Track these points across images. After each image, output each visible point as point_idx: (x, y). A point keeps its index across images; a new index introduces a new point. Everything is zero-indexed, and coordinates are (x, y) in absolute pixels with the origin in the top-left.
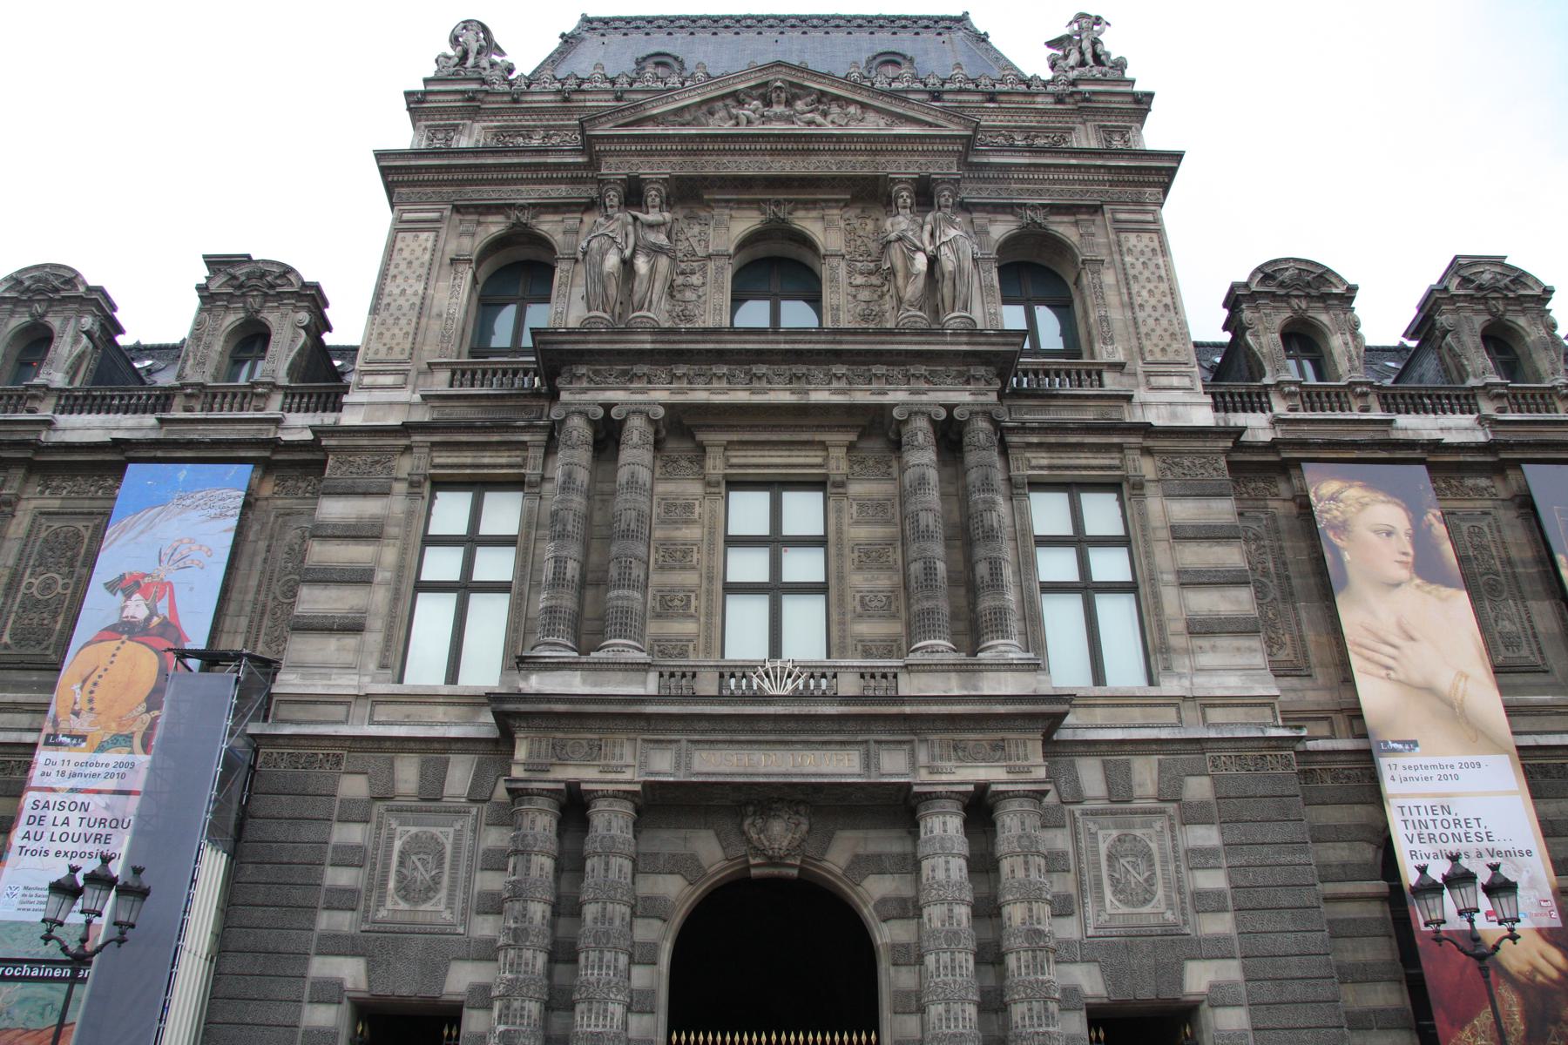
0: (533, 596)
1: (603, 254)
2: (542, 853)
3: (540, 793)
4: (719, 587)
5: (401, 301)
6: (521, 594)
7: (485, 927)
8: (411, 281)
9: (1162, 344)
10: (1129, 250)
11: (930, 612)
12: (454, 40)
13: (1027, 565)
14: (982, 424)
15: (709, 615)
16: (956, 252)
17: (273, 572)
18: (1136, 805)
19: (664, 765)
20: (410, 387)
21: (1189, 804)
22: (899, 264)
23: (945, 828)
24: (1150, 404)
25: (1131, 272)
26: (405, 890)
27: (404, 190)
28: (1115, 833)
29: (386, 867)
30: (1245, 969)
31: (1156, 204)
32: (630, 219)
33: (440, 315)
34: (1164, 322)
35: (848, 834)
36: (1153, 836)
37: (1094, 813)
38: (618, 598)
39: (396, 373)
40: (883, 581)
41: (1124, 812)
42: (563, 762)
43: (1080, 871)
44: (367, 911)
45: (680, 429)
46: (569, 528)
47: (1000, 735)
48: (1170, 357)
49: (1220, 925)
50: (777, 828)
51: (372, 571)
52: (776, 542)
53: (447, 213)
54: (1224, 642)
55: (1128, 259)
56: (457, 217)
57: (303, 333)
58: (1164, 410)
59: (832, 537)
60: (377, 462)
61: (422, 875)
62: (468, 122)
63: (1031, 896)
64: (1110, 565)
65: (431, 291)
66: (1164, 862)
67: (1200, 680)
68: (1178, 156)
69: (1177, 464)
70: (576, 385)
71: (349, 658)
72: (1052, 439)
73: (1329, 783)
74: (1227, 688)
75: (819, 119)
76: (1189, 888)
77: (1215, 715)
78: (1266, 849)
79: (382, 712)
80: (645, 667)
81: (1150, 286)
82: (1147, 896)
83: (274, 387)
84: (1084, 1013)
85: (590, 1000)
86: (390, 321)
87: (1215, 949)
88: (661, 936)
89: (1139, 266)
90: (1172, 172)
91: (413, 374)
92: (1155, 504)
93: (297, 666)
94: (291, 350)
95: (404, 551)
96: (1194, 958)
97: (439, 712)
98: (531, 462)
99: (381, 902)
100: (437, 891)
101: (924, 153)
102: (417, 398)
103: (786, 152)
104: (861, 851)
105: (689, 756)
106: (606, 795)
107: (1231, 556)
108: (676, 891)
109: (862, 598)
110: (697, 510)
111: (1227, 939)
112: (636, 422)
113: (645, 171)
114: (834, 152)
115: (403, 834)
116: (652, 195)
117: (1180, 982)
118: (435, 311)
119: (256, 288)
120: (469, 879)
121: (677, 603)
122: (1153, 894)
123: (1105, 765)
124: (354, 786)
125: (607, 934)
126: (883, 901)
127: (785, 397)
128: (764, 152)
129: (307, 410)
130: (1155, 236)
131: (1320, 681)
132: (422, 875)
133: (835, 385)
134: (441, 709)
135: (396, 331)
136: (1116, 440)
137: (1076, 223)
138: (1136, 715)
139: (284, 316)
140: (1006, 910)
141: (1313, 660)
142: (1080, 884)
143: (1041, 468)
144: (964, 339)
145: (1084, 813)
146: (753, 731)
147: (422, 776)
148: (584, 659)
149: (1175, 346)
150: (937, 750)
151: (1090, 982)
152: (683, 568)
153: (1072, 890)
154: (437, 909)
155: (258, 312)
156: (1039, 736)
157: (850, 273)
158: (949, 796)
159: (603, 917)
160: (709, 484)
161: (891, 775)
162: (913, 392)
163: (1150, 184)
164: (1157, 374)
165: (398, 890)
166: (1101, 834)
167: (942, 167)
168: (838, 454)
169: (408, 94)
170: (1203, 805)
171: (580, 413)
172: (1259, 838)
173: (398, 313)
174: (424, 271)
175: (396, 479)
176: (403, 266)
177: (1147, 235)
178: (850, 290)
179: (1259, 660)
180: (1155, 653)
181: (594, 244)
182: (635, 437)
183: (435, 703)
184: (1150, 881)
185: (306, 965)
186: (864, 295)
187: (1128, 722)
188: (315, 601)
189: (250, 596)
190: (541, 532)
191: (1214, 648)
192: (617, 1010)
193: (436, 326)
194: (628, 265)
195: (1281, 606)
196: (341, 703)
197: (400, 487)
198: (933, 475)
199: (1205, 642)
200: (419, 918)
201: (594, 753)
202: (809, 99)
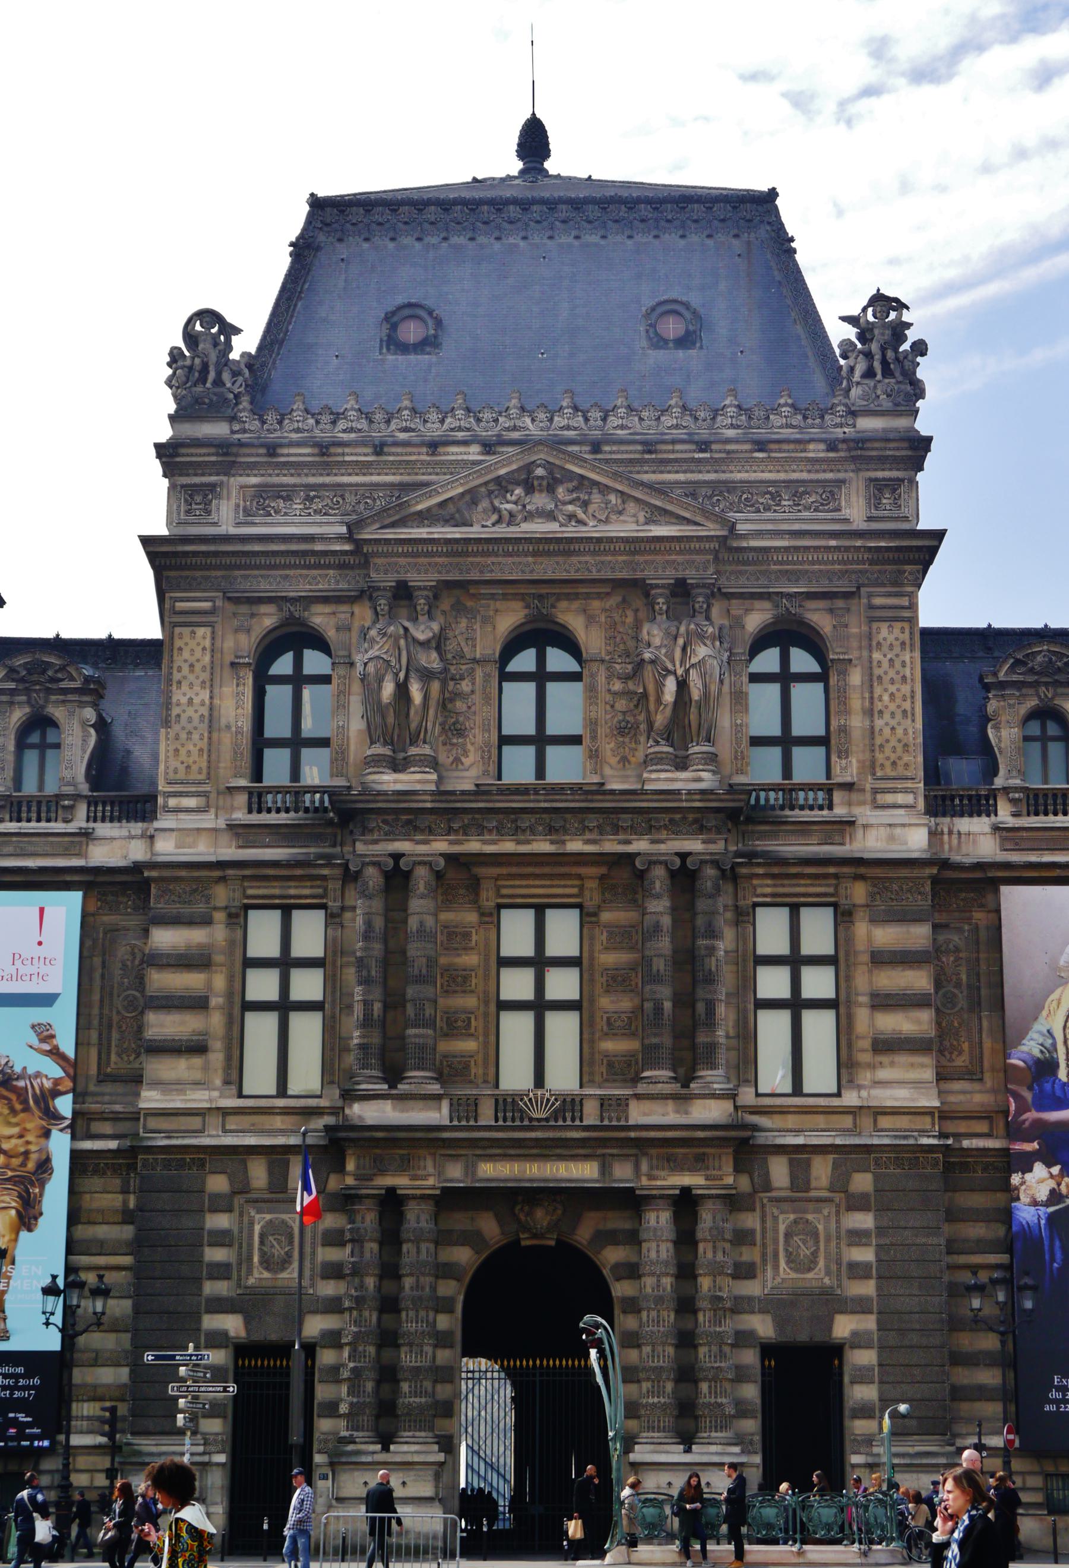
0: (343, 1017)
1: (380, 680)
2: (371, 1240)
3: (368, 1196)
4: (493, 1008)
5: (190, 712)
6: (333, 1017)
7: (328, 1289)
8: (197, 688)
9: (893, 757)
10: (879, 644)
11: (657, 1047)
12: (189, 336)
14: (710, 872)
15: (486, 1035)
16: (703, 676)
17: (112, 987)
18: (813, 1194)
19: (455, 1174)
20: (213, 810)
21: (853, 1195)
22: (651, 688)
24: (871, 826)
25: (877, 672)
26: (267, 1262)
27: (172, 573)
28: (792, 1217)
29: (250, 1245)
30: (879, 1322)
31: (913, 585)
32: (402, 631)
33: (228, 727)
34: (900, 731)
35: (592, 1214)
36: (819, 1220)
37: (778, 1200)
38: (416, 1036)
39: (197, 794)
40: (626, 1004)
41: (800, 1200)
42: (382, 1172)
43: (764, 1245)
44: (239, 1279)
45: (460, 876)
46: (373, 973)
47: (702, 1150)
48: (900, 771)
49: (867, 1288)
50: (539, 1213)
51: (207, 998)
52: (540, 963)
53: (219, 603)
54: (903, 1059)
55: (876, 656)
56: (230, 607)
57: (92, 731)
58: (883, 832)
59: (585, 962)
60: (195, 891)
61: (278, 1251)
62: (224, 478)
63: (717, 1271)
64: (818, 983)
65: (216, 701)
66: (828, 1239)
67: (875, 1092)
69: (886, 888)
70: (368, 837)
71: (198, 1075)
72: (776, 870)
73: (980, 1174)
74: (896, 1099)
75: (581, 515)
76: (845, 1260)
77: (885, 1122)
78: (906, 1233)
79: (232, 1123)
80: (438, 1098)
81: (892, 689)
82: (810, 1264)
83: (77, 797)
84: (758, 1349)
85: (411, 1345)
86: (183, 736)
87: (860, 1306)
89: (885, 664)
90: (933, 551)
91: (213, 796)
92: (861, 928)
93: (157, 1084)
94: (84, 751)
95: (231, 979)
96: (842, 1312)
97: (278, 1122)
98: (331, 894)
99: (250, 1272)
100: (290, 1263)
101: (680, 552)
102: (221, 823)
103: (548, 554)
104: (601, 1227)
105: (475, 1166)
106: (414, 1197)
107: (919, 980)
109: (608, 1019)
110: (474, 938)
111: (869, 1299)
112: (421, 872)
113: (415, 578)
114: (594, 553)
115: (260, 1220)
117: (830, 1329)
118: (223, 722)
119: (38, 683)
120: (314, 1253)
121: (460, 1023)
122: (816, 1263)
123: (791, 1163)
124: (217, 1183)
125: (420, 1298)
126: (616, 1267)
127: (543, 846)
128: (526, 554)
129: (111, 821)
130: (906, 625)
131: (989, 1084)
132: (278, 1251)
133: (588, 836)
134: (278, 1118)
135: (191, 748)
136: (832, 870)
137: (831, 611)
138: (821, 1120)
139: (71, 714)
140: (700, 1279)
141: (986, 1065)
142: (764, 1255)
143: (765, 896)
144: (697, 797)
145: (771, 1200)
146: (520, 1147)
147: (270, 1173)
148: (394, 1092)
149: (906, 758)
150: (654, 1162)
151: (763, 1326)
152: (464, 992)
153: (758, 1259)
155: (43, 707)
156: (731, 1150)
157: (609, 678)
158: (662, 1197)
159: (417, 1286)
160: (482, 915)
161: (621, 1181)
162: (653, 842)
163: (909, 562)
164: (885, 791)
165: (261, 1263)
166: (781, 1217)
167: (697, 570)
169: (158, 446)
170: (865, 1196)
171: (373, 864)
172: (902, 1224)
173: (189, 727)
174: (205, 676)
175: (215, 908)
176: (186, 669)
177: (898, 625)
178: (609, 697)
179: (929, 1074)
180: (846, 1066)
181: (371, 668)
182: (421, 888)
183: (273, 1114)
184: (815, 1254)
185: (199, 1321)
186: (621, 704)
187: (812, 1127)
188: (163, 1025)
189: (96, 1011)
190: (345, 959)
191: (892, 1064)
192: (428, 1349)
194: (402, 690)
195: (966, 1016)
196: (197, 1114)
197: (220, 916)
198: (666, 921)
199: (885, 1059)
200: (279, 1283)
201: (405, 1165)
202: (570, 485)
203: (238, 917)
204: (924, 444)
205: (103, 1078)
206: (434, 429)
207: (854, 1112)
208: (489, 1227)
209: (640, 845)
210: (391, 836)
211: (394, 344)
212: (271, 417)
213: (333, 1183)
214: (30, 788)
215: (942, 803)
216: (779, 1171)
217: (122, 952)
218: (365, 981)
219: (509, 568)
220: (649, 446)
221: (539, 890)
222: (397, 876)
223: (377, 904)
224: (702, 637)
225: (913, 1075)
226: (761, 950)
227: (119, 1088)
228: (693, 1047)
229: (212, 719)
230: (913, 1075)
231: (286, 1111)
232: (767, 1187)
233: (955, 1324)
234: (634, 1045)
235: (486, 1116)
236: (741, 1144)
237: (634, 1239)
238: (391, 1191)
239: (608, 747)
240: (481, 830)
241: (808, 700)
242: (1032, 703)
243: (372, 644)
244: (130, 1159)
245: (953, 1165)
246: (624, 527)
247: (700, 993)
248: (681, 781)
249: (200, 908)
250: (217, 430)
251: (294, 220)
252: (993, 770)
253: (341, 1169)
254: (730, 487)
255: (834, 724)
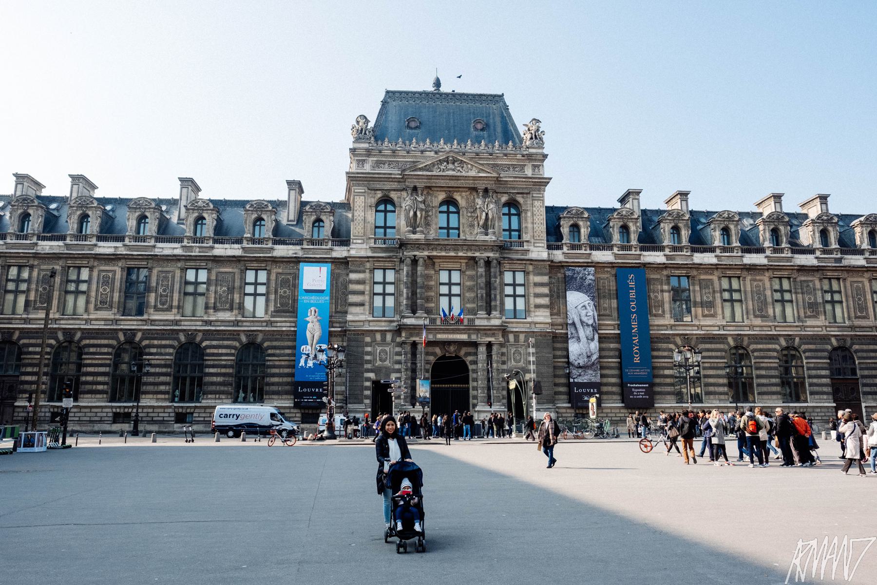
7: (397, 366)
13: (502, 291)
14: (495, 261)
19: (431, 337)
23: (482, 349)
26: (381, 360)
40: (473, 295)
42: (412, 336)
54: (542, 310)
64: (520, 291)
68: (550, 179)
77: (537, 326)
79: (371, 324)
88: (429, 367)
92: (531, 277)
93: (351, 314)
97: (383, 324)
108: (432, 359)
113: (418, 185)
115: (379, 349)
116: (420, 192)
124: (368, 339)
127: (452, 254)
132: (384, 357)
138: (522, 325)
154: (387, 363)
167: (491, 185)
168: (464, 264)
179: (548, 314)
186: (470, 219)
188: (352, 299)
193: (369, 225)
194: (415, 213)
197: (368, 271)
203: (372, 271)
204: (545, 156)
205: (336, 312)
206: (422, 148)
207: (530, 323)
208: (438, 350)
209: (477, 254)
210: (413, 250)
211: (408, 127)
212: (379, 143)
213: (398, 340)
214: (315, 237)
215: (549, 247)
216: (511, 337)
217: (341, 279)
218: (407, 288)
219: (442, 183)
220: (477, 154)
221: (450, 266)
222: (415, 261)
223: (410, 268)
224: (492, 202)
225: (545, 314)
226: (506, 282)
227: (340, 315)
228: (490, 306)
229: (365, 220)
230: (545, 314)
231: (385, 321)
232: (508, 341)
233: (555, 376)
234: (475, 305)
235: (438, 322)
236: (503, 330)
237: (476, 354)
238: (414, 341)
239: (467, 230)
240: (436, 249)
241: (514, 219)
242: (572, 222)
243: (406, 201)
244: (344, 333)
245: (555, 337)
246: (473, 173)
247: (493, 292)
248: (487, 238)
249: (362, 269)
250: (366, 145)
251: (382, 96)
252: (562, 239)
253: (400, 336)
254: (497, 165)
255: (524, 226)
